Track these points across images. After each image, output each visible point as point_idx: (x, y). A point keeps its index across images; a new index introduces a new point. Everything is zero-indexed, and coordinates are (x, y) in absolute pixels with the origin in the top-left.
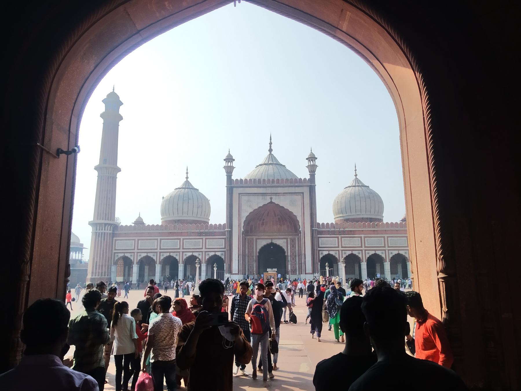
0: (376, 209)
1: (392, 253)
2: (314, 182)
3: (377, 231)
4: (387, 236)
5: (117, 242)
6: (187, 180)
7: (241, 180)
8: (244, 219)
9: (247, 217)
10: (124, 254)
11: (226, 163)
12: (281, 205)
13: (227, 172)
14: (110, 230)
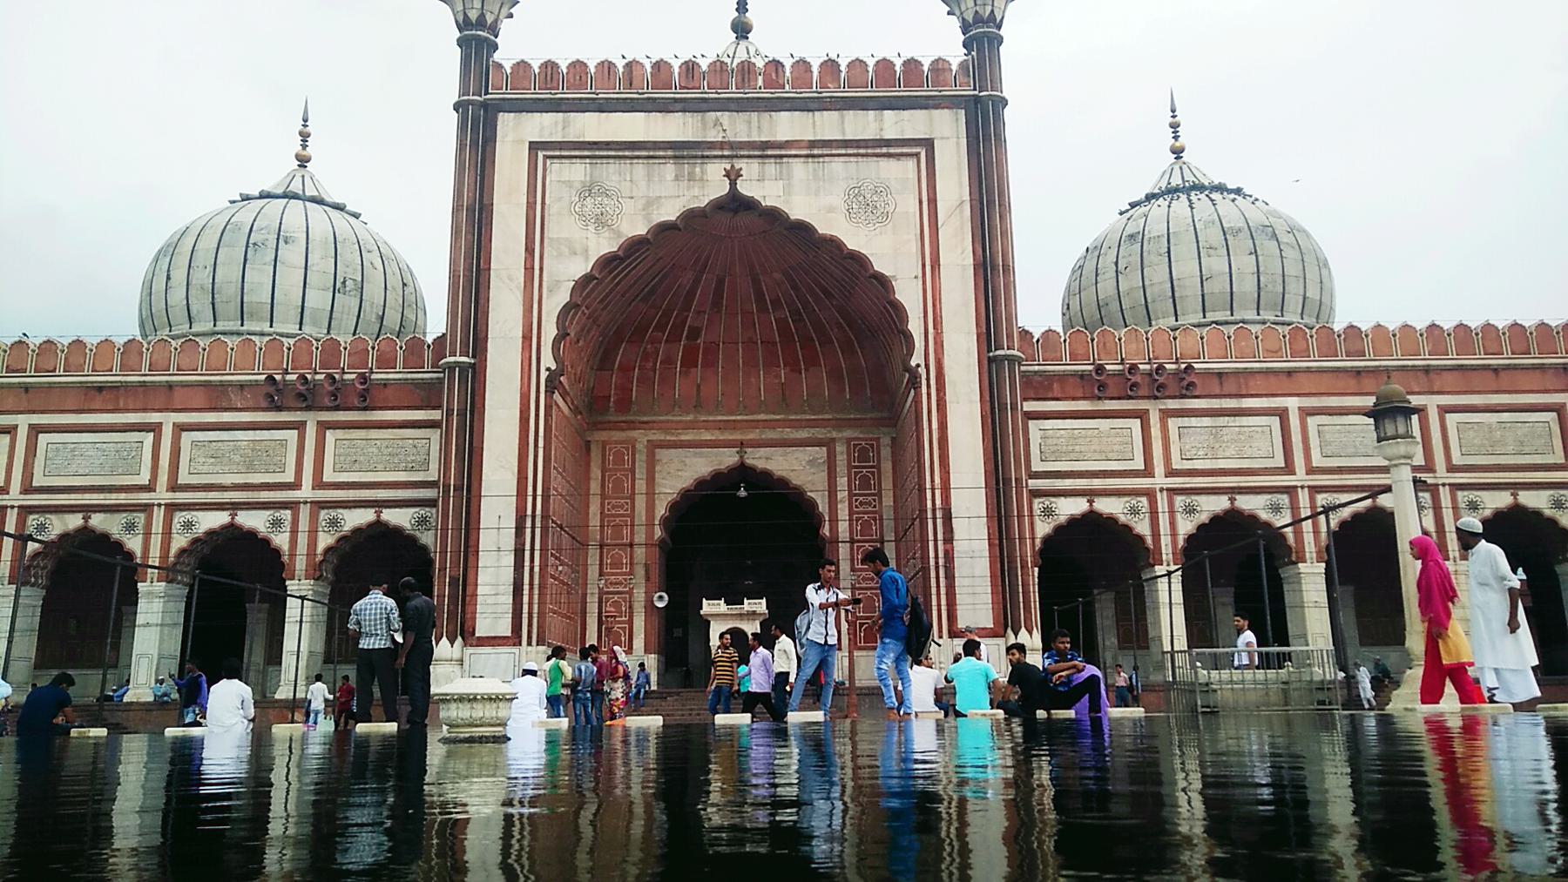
2: (996, 83)
3: (1374, 371)
4: (1438, 406)
8: (555, 301)
9: (583, 284)
12: (792, 218)
13: (464, 24)
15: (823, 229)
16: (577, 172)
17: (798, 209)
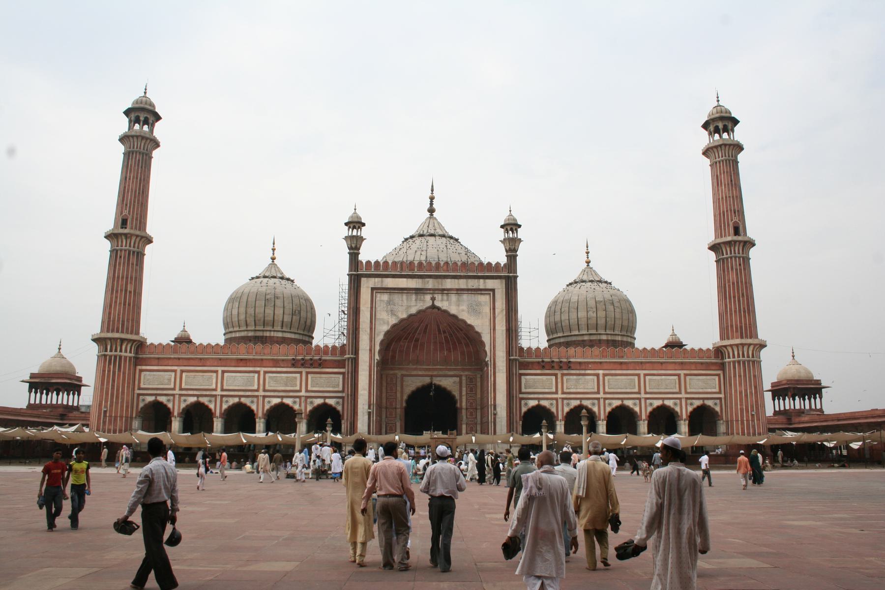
0: (623, 324)
1: (651, 404)
2: (515, 272)
3: (625, 363)
5: (143, 374)
6: (273, 262)
7: (377, 263)
8: (379, 338)
9: (387, 334)
10: (156, 397)
11: (349, 230)
13: (350, 248)
14: (130, 352)
15: (461, 317)
16: (385, 297)
17: (453, 310)
